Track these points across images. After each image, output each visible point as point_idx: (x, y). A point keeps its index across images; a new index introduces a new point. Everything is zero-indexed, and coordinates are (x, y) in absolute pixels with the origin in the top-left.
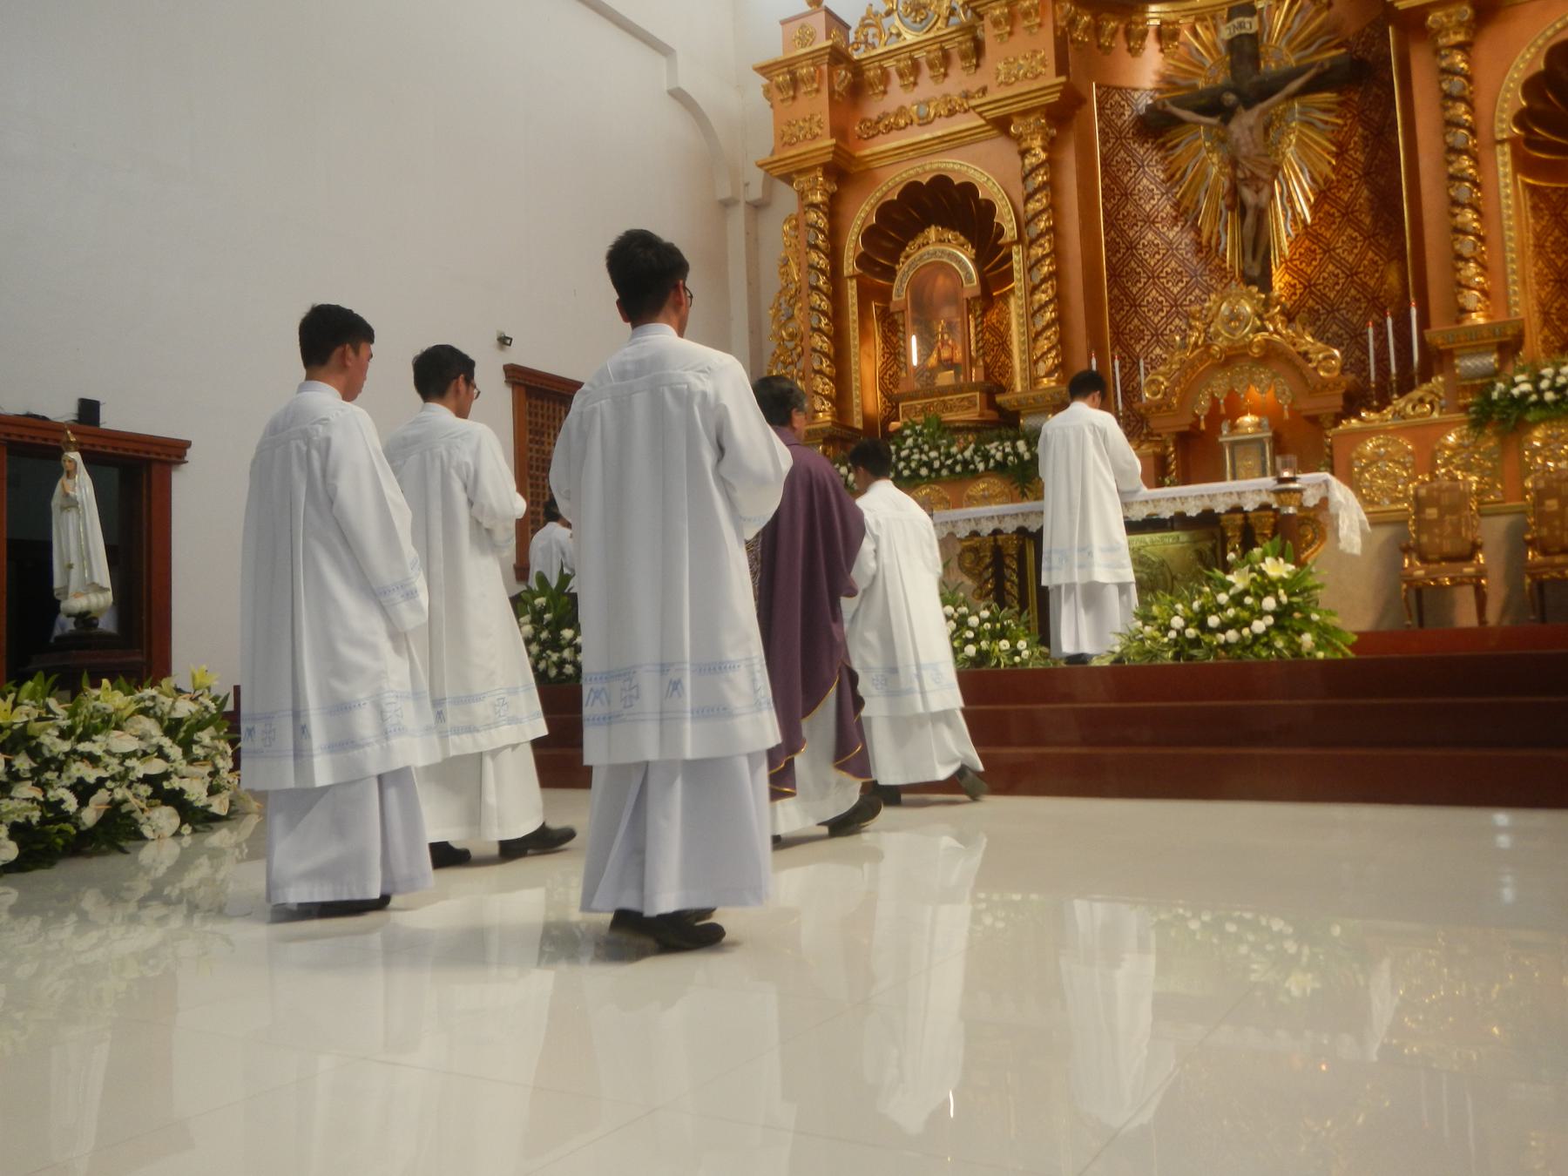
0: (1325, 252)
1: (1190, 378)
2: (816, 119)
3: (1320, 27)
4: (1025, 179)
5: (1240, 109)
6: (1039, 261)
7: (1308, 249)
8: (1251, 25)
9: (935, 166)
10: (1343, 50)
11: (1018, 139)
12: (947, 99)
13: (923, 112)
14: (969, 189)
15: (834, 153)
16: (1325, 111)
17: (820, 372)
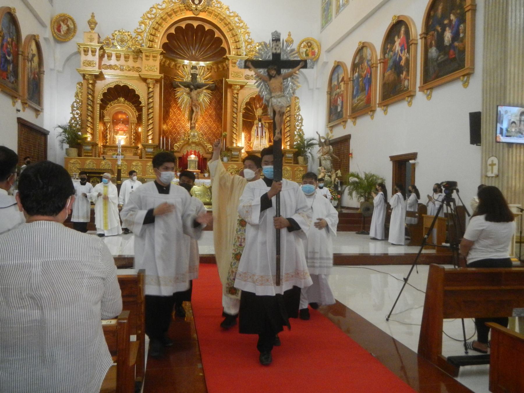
0: (205, 122)
1: (182, 147)
2: (95, 62)
3: (210, 77)
4: (149, 93)
5: (194, 90)
6: (151, 113)
7: (202, 120)
8: (197, 72)
9: (125, 83)
10: (213, 82)
11: (148, 84)
12: (128, 67)
13: (122, 68)
14: (133, 91)
15: (100, 73)
16: (209, 94)
17: (89, 127)
